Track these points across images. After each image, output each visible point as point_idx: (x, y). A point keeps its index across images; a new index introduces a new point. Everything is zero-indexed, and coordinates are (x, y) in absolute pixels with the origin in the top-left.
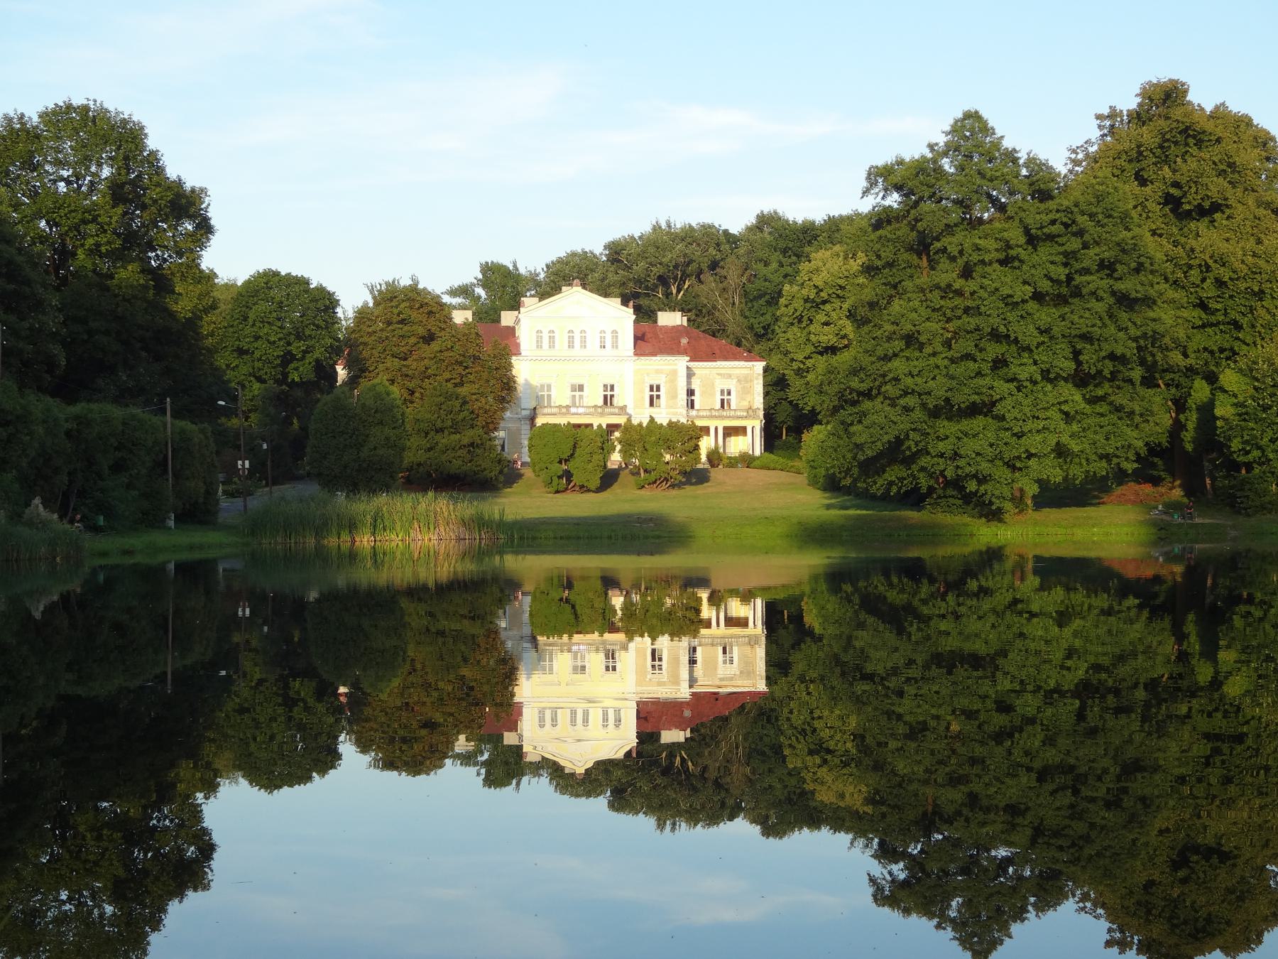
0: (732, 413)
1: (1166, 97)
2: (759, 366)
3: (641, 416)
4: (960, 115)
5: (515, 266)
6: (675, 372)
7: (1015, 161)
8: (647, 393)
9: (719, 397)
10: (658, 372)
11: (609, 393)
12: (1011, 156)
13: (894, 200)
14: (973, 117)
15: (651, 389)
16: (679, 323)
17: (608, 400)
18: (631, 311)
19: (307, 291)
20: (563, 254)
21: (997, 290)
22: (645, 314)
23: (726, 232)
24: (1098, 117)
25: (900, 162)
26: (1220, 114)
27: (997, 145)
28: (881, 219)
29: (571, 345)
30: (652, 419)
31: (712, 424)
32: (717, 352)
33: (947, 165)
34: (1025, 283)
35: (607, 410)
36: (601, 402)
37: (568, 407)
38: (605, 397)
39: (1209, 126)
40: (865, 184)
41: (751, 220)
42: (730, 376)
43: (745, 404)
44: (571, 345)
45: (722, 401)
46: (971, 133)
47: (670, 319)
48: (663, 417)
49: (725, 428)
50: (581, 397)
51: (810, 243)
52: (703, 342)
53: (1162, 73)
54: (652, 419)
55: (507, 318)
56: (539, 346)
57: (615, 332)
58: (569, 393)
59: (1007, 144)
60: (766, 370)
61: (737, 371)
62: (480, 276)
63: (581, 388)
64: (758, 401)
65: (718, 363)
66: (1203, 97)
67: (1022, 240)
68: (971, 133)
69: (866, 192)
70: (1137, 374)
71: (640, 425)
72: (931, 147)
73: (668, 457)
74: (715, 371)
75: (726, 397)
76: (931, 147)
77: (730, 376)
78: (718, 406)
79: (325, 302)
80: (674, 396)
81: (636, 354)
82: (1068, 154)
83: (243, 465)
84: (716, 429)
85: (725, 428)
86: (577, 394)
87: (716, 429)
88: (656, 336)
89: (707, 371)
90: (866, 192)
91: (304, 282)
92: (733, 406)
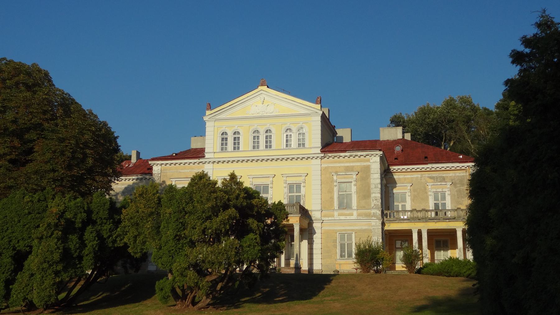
6: (367, 169)
10: (348, 169)
16: (400, 136)
29: (256, 147)
31: (414, 227)
42: (443, 179)
44: (256, 147)
45: (436, 205)
61: (451, 174)
65: (430, 166)
74: (427, 174)
77: (443, 179)
81: (323, 151)
84: (420, 233)
87: (420, 233)
89: (418, 175)
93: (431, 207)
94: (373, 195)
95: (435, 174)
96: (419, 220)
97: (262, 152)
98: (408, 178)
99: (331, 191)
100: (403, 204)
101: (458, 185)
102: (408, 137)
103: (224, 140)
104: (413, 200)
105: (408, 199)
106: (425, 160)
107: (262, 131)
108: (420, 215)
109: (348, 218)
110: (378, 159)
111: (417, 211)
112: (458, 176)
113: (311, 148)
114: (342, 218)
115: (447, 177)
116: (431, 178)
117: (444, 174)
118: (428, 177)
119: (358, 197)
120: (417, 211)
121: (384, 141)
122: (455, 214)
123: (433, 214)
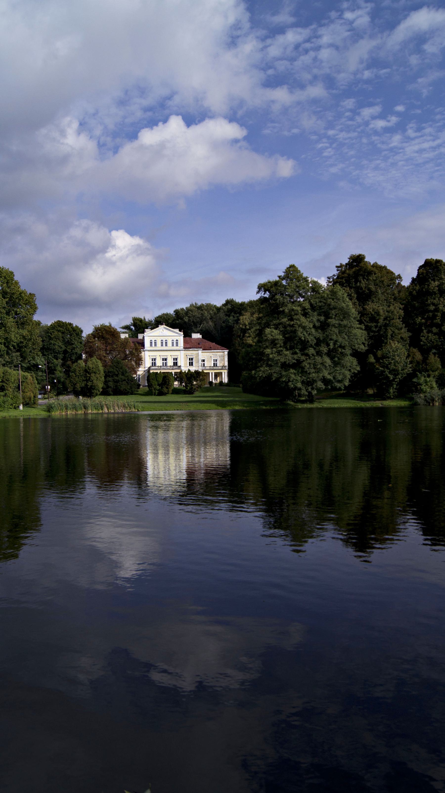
0: (217, 368)
1: (357, 260)
2: (226, 352)
3: (185, 369)
4: (288, 266)
5: (144, 319)
7: (307, 281)
8: (188, 361)
9: (213, 362)
11: (175, 361)
12: (306, 279)
13: (267, 295)
14: (292, 266)
15: (190, 360)
17: (175, 364)
18: (182, 333)
19: (72, 328)
20: (160, 314)
21: (301, 324)
22: (187, 335)
23: (215, 306)
24: (337, 267)
25: (269, 282)
26: (376, 266)
27: (301, 275)
28: (263, 300)
29: (162, 345)
30: (189, 370)
32: (212, 347)
33: (284, 282)
34: (310, 322)
35: (175, 367)
36: (172, 364)
37: (161, 366)
38: (174, 362)
39: (372, 269)
40: (257, 290)
41: (224, 302)
43: (221, 365)
45: (214, 363)
46: (292, 272)
47: (196, 336)
48: (193, 369)
49: (215, 373)
50: (166, 363)
51: (243, 310)
52: (207, 344)
53: (356, 252)
54: (189, 370)
55: (140, 336)
56: (151, 345)
57: (177, 340)
58: (162, 362)
59: (304, 275)
61: (219, 353)
62: (132, 322)
63: (166, 359)
64: (226, 364)
66: (370, 259)
67: (309, 307)
68: (292, 272)
69: (258, 292)
70: (348, 351)
71: (185, 372)
72: (279, 277)
73: (195, 383)
74: (211, 353)
75: (215, 362)
76: (279, 277)
78: (213, 365)
79: (77, 331)
81: (184, 348)
82: (327, 279)
83: (48, 387)
84: (212, 373)
85: (215, 373)
86: (164, 362)
87: (212, 373)
88: (191, 342)
89: (209, 354)
90: (258, 292)
91: (70, 324)
92: (218, 365)
95: (214, 353)
96: (212, 369)
97: (164, 348)
99: (186, 361)
103: (151, 343)
105: (205, 361)
106: (210, 349)
117: (217, 354)
122: (220, 368)
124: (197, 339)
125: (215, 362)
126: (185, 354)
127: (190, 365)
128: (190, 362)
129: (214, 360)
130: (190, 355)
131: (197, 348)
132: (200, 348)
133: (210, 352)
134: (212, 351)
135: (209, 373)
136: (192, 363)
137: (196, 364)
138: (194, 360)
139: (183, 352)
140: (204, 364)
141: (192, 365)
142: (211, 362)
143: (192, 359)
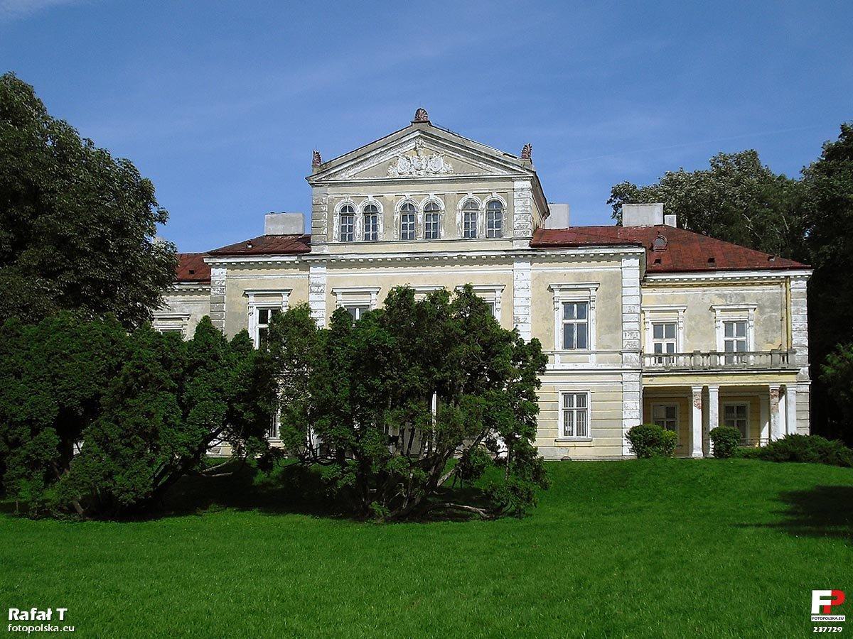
6: (617, 280)
45: (728, 344)
56: (346, 238)
57: (494, 204)
60: (811, 283)
61: (757, 290)
77: (743, 298)
80: (615, 323)
89: (698, 291)
93: (721, 348)
94: (626, 326)
96: (706, 372)
98: (679, 296)
99: (551, 319)
100: (670, 341)
101: (768, 310)
102: (671, 220)
104: (687, 336)
106: (710, 265)
107: (421, 206)
108: (706, 362)
109: (580, 366)
110: (636, 262)
111: (703, 355)
112: (769, 293)
113: (511, 240)
114: (571, 366)
115: (749, 294)
116: (720, 296)
118: (716, 294)
119: (598, 330)
120: (703, 355)
121: (630, 228)
122: (764, 361)
123: (722, 360)
124: (648, 228)
125: (735, 339)
126: (538, 278)
127: (568, 344)
128: (568, 329)
129: (728, 324)
130: (566, 282)
131: (610, 245)
132: (632, 244)
133: (709, 284)
134: (719, 275)
135: (687, 391)
136: (583, 329)
137: (607, 339)
138: (592, 314)
139: (524, 272)
140: (670, 346)
141: (582, 343)
142: (712, 335)
143: (583, 307)
